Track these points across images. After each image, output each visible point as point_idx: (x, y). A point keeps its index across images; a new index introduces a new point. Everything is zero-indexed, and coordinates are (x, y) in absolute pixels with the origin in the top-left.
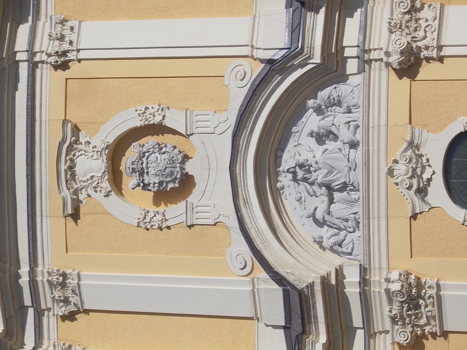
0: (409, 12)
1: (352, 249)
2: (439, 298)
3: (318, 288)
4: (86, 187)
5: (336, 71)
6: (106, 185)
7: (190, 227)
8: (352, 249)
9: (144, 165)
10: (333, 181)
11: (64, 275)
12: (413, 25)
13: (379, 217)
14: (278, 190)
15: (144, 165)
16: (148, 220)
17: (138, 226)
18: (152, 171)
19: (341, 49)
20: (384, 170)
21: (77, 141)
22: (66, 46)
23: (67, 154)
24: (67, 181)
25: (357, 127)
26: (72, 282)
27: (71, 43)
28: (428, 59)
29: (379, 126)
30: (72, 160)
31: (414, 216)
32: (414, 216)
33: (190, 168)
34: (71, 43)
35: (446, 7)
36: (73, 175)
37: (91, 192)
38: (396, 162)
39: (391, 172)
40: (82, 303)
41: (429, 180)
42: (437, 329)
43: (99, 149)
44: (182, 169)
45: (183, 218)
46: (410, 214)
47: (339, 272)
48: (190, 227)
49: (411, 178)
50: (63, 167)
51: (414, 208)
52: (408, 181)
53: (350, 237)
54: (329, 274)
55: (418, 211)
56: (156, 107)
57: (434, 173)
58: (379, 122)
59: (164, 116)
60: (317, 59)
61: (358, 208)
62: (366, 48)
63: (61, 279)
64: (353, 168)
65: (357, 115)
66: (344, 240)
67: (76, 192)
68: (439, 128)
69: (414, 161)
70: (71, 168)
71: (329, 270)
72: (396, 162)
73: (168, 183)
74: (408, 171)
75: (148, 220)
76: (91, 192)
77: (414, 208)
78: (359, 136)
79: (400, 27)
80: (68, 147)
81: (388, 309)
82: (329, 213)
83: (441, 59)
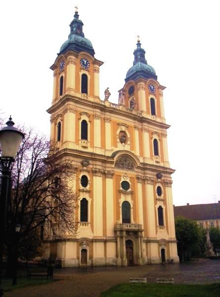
39: (126, 174)
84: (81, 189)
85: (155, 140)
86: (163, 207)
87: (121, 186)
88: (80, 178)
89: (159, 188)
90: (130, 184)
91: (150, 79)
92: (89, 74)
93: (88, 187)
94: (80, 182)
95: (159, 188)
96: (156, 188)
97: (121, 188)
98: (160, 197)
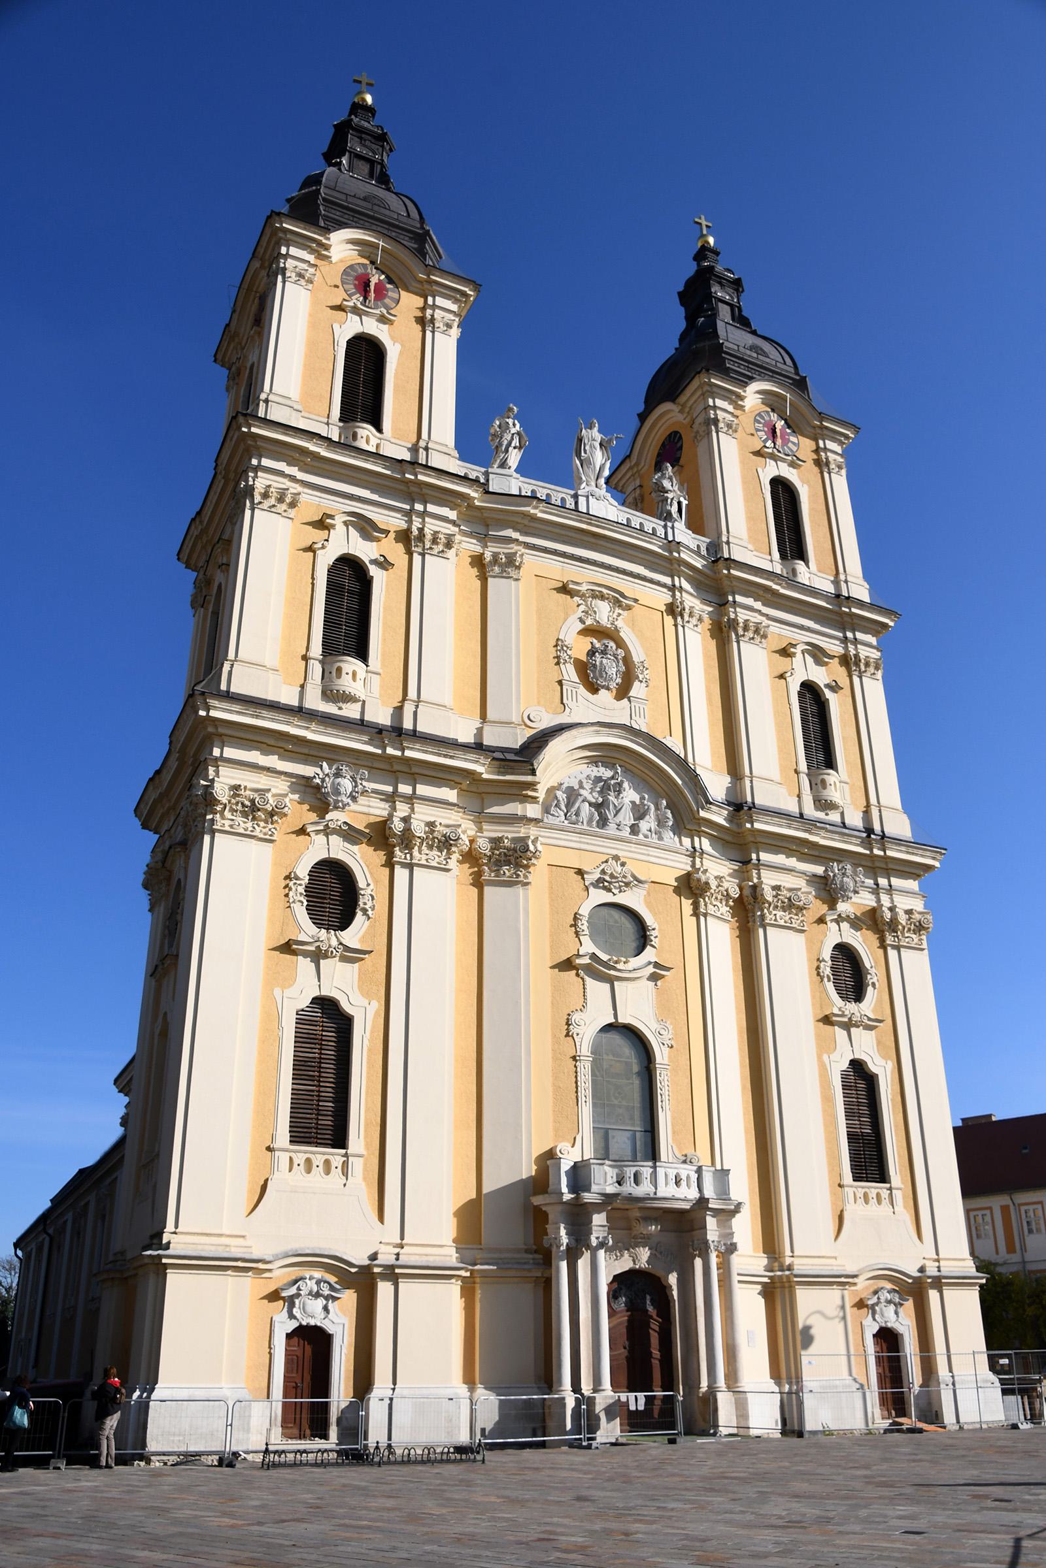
0: (728, 894)
1: (553, 815)
2: (517, 883)
3: (529, 778)
4: (587, 606)
5: (685, 828)
6: (589, 622)
7: (560, 683)
8: (553, 815)
9: (609, 656)
10: (609, 810)
11: (518, 568)
12: (719, 897)
13: (580, 842)
14: (596, 763)
15: (609, 656)
16: (565, 648)
17: (558, 640)
18: (605, 661)
19: (700, 834)
20: (620, 854)
21: (620, 607)
22: (686, 618)
23: (613, 596)
24: (592, 590)
25: (646, 836)
26: (513, 573)
27: (688, 622)
28: (696, 906)
29: (648, 855)
30: (608, 599)
31: (580, 872)
32: (580, 872)
33: (603, 692)
34: (688, 622)
35: (728, 925)
36: (594, 597)
37: (583, 608)
38: (623, 864)
39: (616, 858)
40: (494, 577)
41: (609, 890)
42: (486, 876)
43: (616, 623)
44: (603, 687)
45: (566, 677)
46: (585, 869)
47: (534, 799)
48: (560, 683)
49: (612, 876)
50: (605, 591)
51: (587, 873)
52: (609, 872)
53: (562, 814)
54: (535, 790)
55: (585, 876)
56: (647, 677)
57: (614, 894)
58: (652, 856)
59: (641, 682)
60: (703, 814)
61: (585, 827)
62: (705, 856)
63: (517, 564)
64: (620, 828)
65: (654, 839)
66: (560, 809)
67: (582, 596)
68: (648, 905)
69: (624, 880)
70: (602, 597)
71: (539, 791)
72: (623, 864)
73: (594, 672)
74: (617, 873)
75: (565, 648)
76: (583, 608)
77: (587, 873)
78: (641, 836)
79: (720, 885)
80: (617, 598)
81: (509, 837)
82: (583, 801)
83: (696, 913)
84: (302, 937)
85: (809, 690)
86: (880, 1067)
87: (584, 925)
88: (303, 872)
89: (845, 952)
90: (649, 920)
91: (755, 386)
92: (394, 339)
93: (353, 936)
94: (298, 891)
95: (845, 952)
96: (827, 953)
97: (588, 946)
98: (851, 1008)
